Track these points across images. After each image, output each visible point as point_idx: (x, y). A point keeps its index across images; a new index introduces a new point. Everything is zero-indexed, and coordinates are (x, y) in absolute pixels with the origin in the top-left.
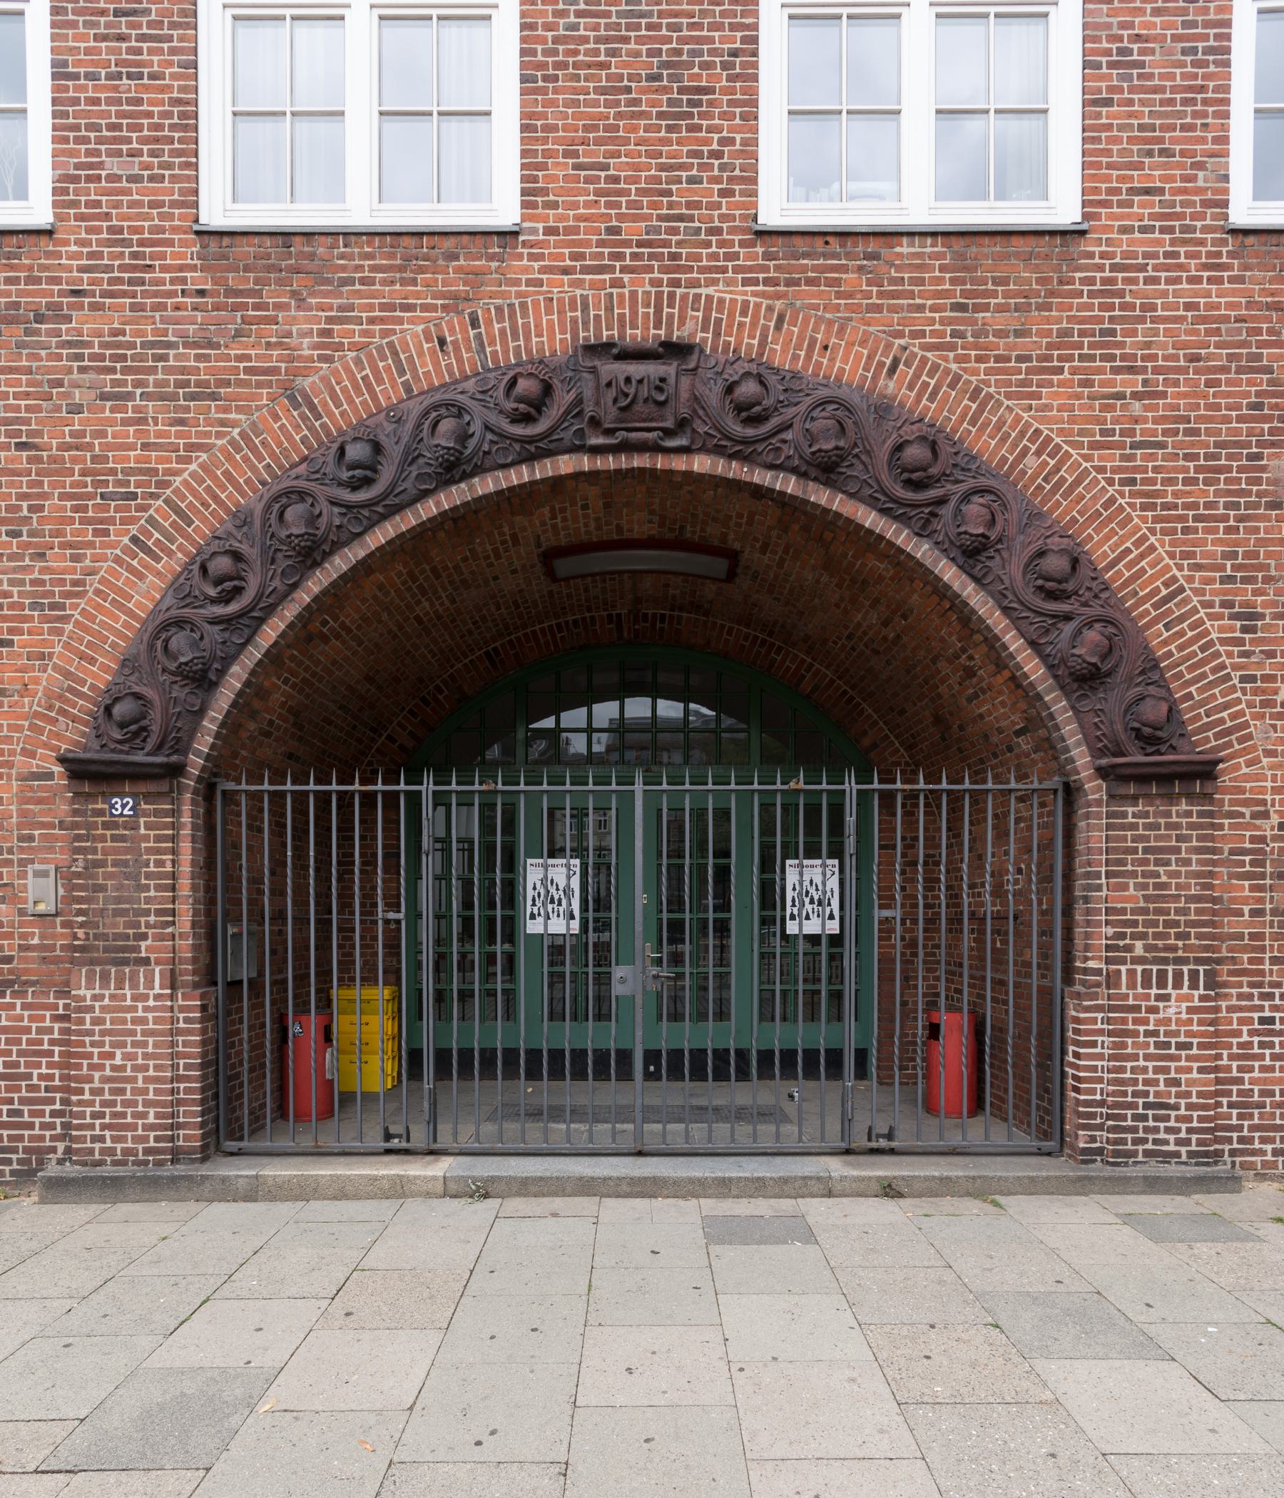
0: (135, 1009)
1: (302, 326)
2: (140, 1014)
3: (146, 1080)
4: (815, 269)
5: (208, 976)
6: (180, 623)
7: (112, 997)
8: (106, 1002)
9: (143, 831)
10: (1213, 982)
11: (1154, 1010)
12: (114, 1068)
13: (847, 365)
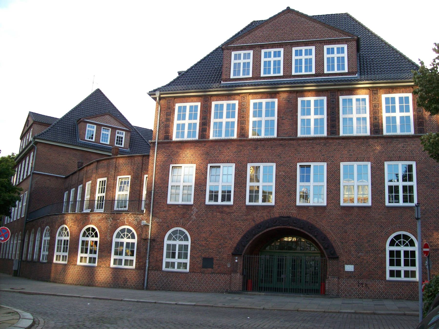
1: (255, 214)
5: (243, 274)
10: (338, 278)
13: (304, 218)
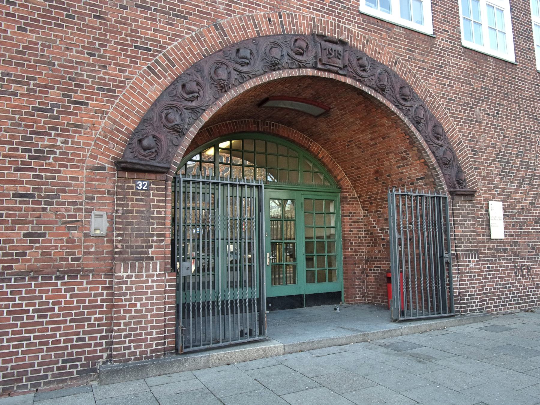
0: (147, 281)
2: (150, 284)
3: (152, 316)
4: (375, 28)
6: (171, 107)
7: (137, 276)
8: (134, 278)
9: (151, 197)
11: (468, 265)
12: (136, 311)
13: (384, 59)
